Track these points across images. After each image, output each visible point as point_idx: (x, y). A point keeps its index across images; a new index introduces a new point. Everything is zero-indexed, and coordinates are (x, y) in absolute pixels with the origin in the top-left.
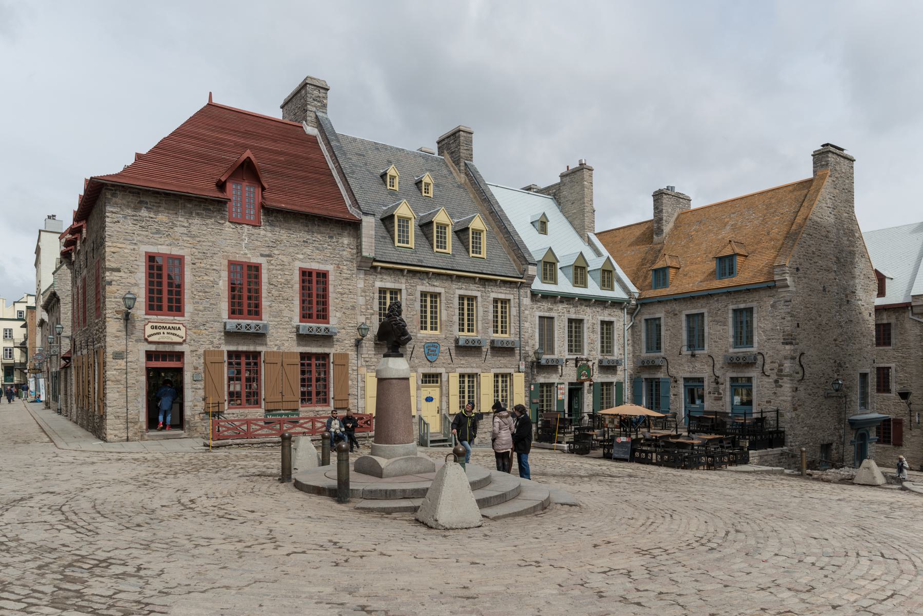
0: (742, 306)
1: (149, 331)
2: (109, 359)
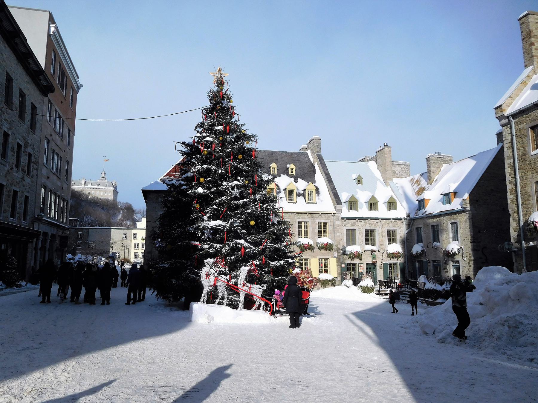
0: (453, 221)
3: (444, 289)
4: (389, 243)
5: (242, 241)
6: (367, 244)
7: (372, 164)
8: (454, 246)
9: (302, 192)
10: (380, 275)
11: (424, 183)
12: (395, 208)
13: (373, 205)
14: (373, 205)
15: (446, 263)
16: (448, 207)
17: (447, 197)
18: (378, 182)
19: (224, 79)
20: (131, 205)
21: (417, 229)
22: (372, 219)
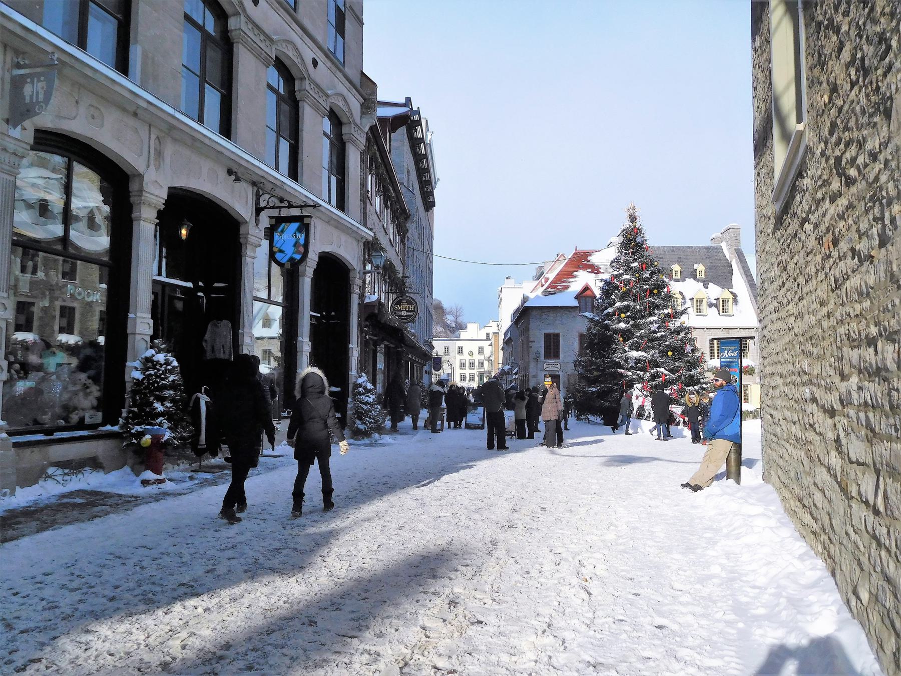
1: (545, 366)
2: (530, 378)
5: (662, 370)
9: (714, 302)
19: (637, 214)
20: (440, 302)
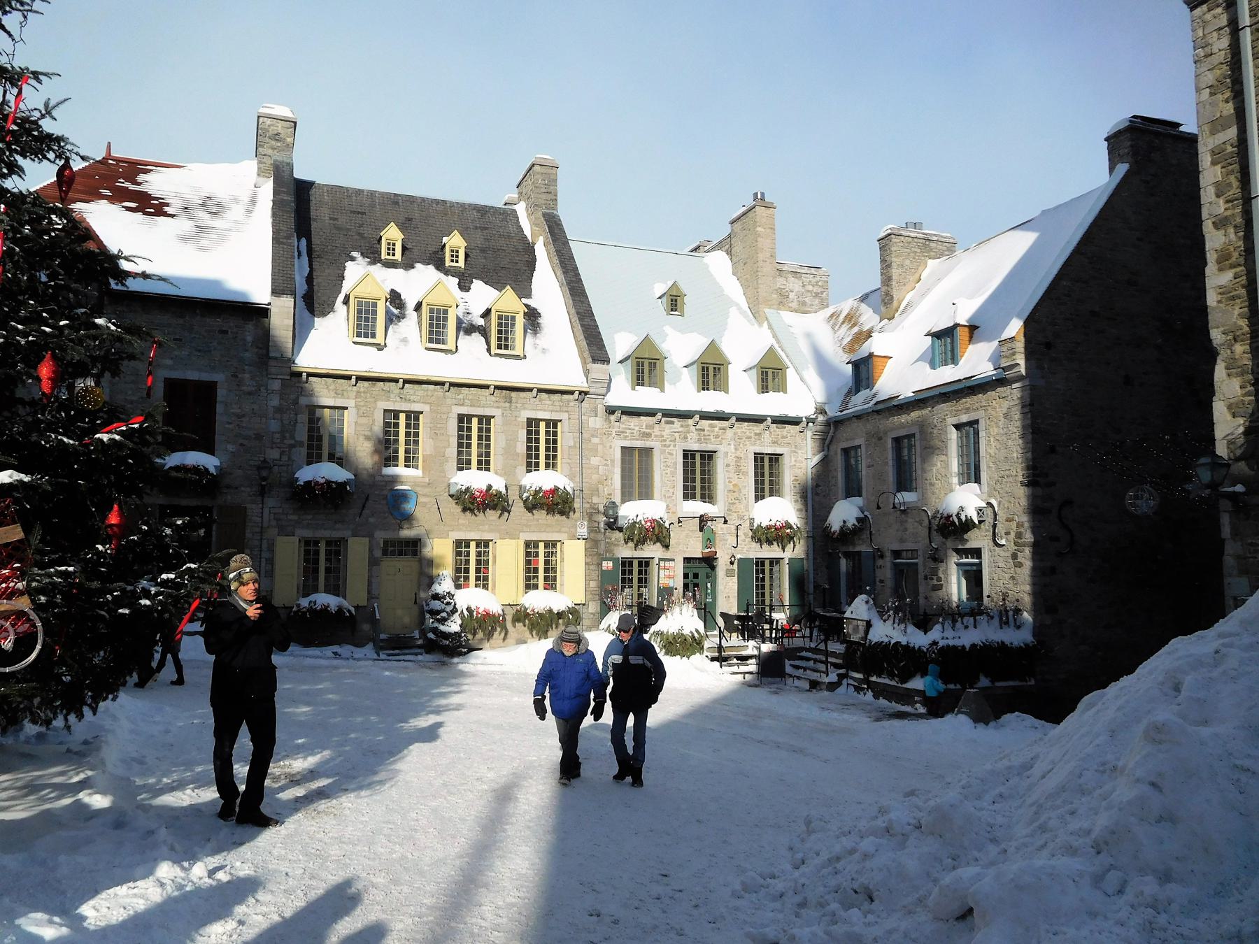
0: (964, 418)
3: (935, 643)
4: (759, 496)
6: (688, 495)
7: (719, 262)
8: (966, 500)
9: (481, 322)
10: (727, 597)
11: (868, 318)
12: (781, 388)
13: (711, 372)
14: (711, 372)
15: (937, 558)
16: (948, 374)
17: (946, 341)
18: (733, 310)
21: (846, 451)
22: (705, 416)
